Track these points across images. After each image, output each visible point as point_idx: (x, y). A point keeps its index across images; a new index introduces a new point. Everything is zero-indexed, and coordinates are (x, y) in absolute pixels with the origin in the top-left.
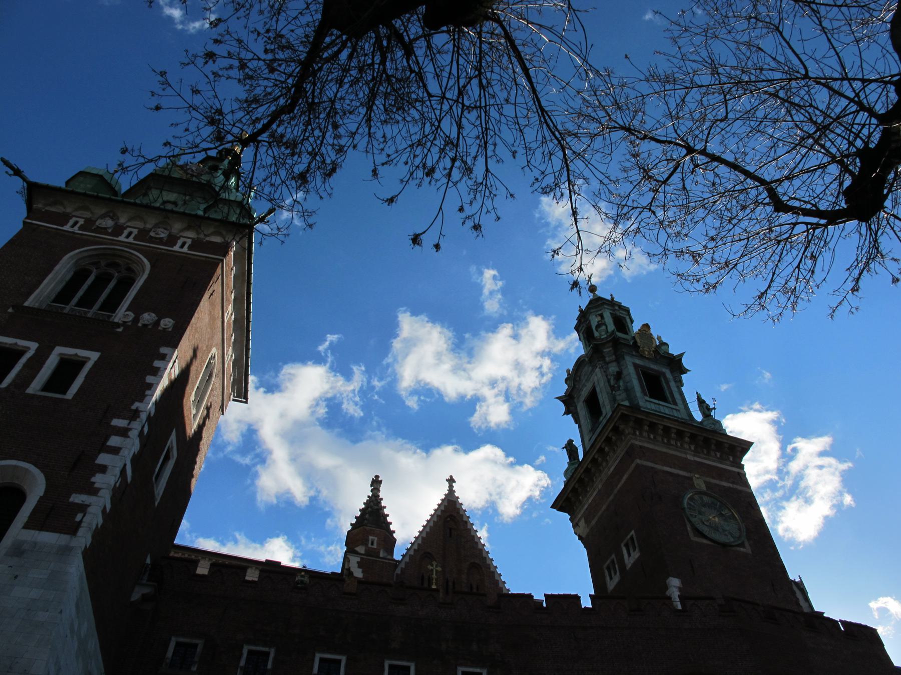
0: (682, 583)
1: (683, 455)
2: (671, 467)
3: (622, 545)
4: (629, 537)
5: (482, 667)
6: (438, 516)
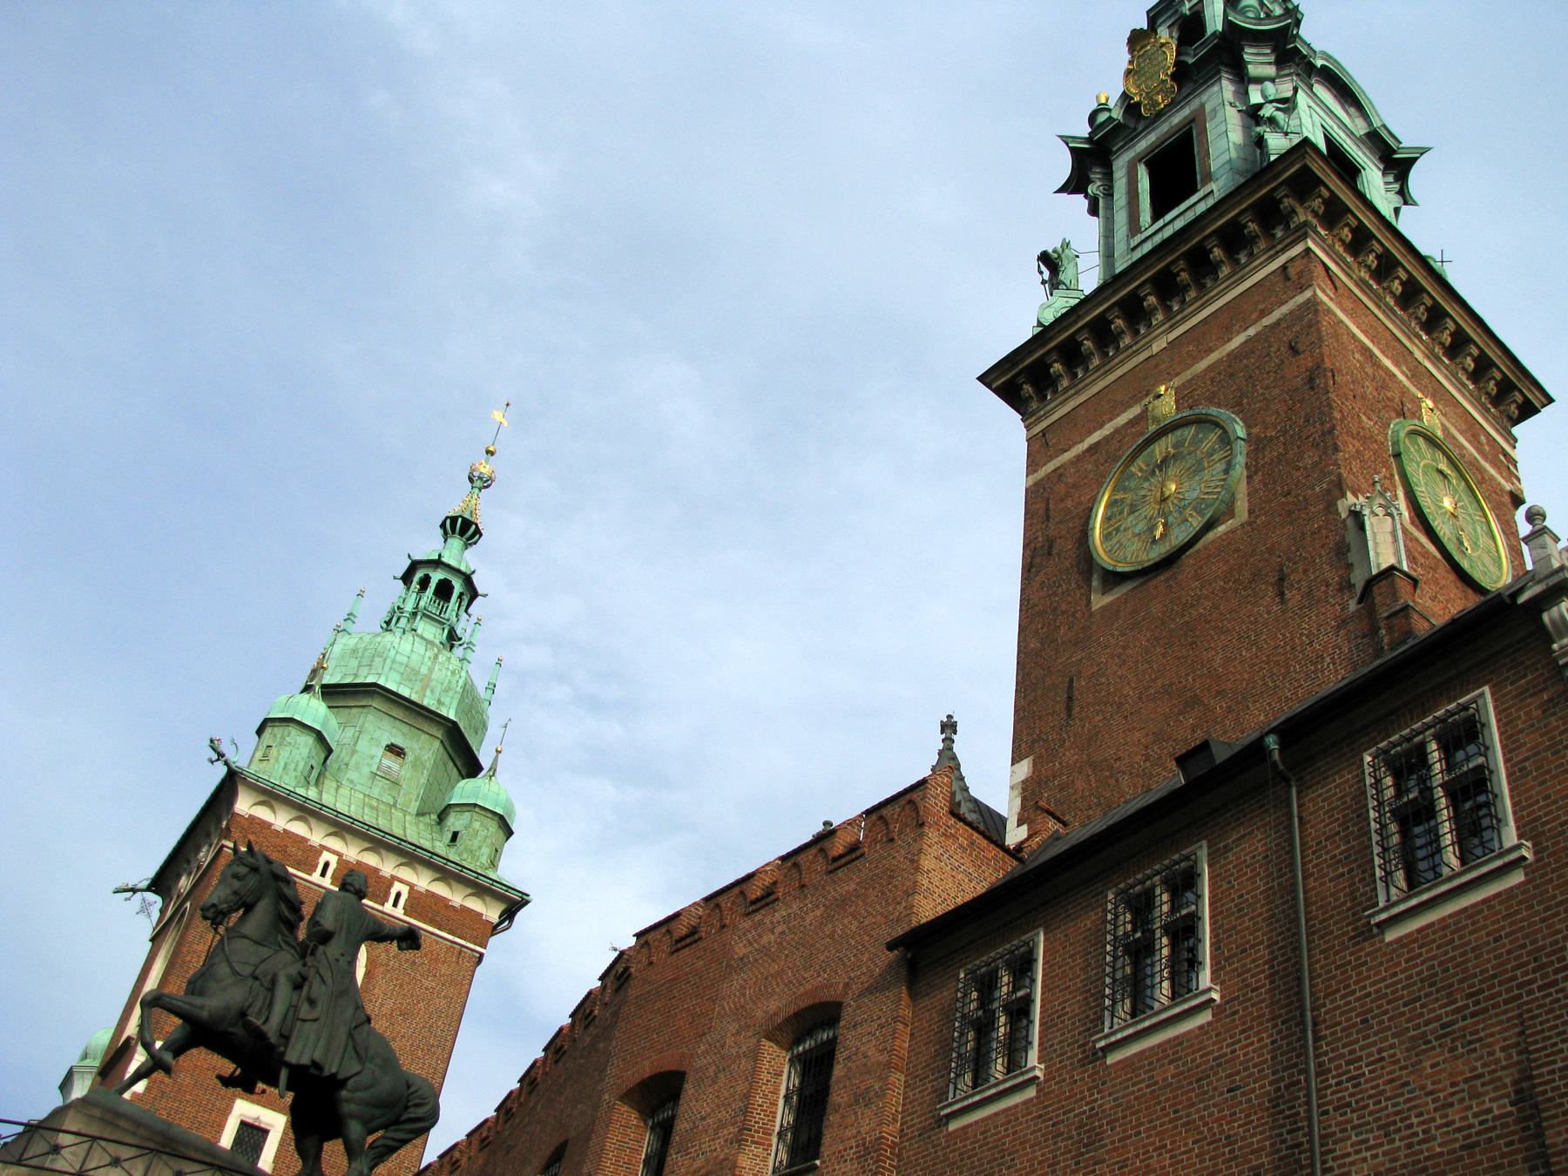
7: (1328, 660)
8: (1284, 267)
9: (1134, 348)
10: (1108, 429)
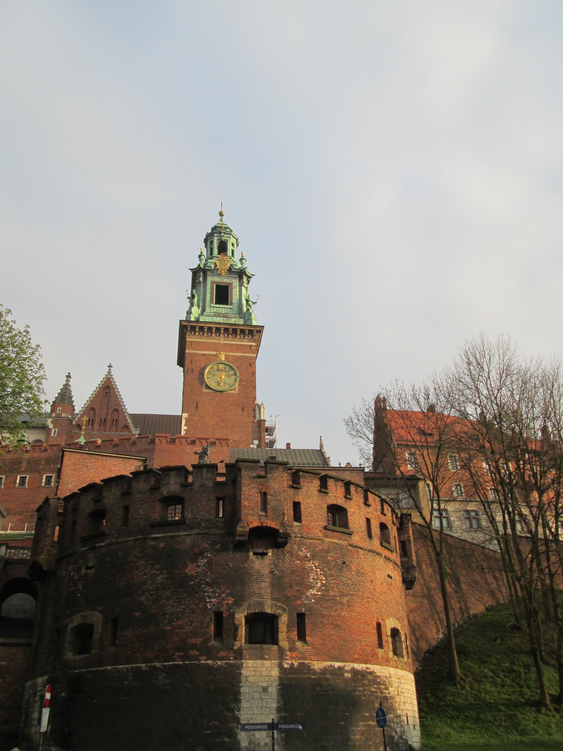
1: (217, 342)
2: (206, 351)
5: (53, 473)
6: (100, 388)
8: (250, 346)
10: (208, 353)
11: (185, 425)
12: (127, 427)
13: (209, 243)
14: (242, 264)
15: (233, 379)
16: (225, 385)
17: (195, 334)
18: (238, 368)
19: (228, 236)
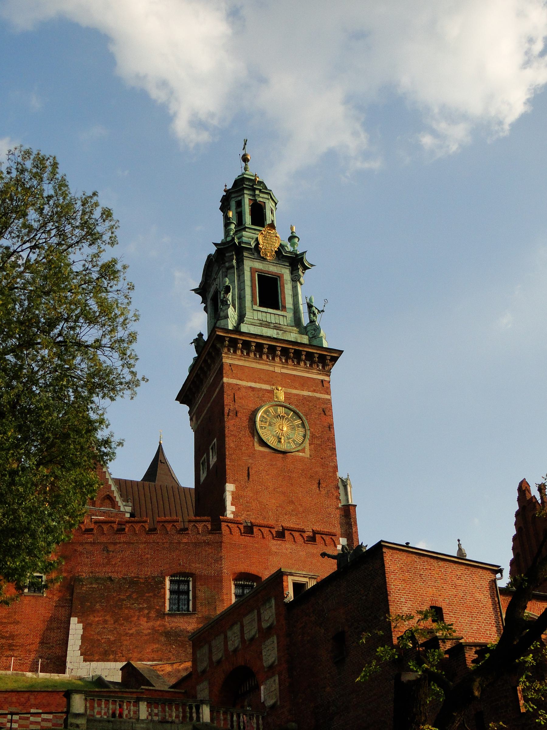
0: (236, 487)
1: (271, 369)
2: (255, 382)
3: (210, 448)
4: (213, 442)
7: (332, 516)
8: (322, 381)
9: (269, 363)
11: (232, 504)
12: (110, 498)
13: (233, 204)
14: (293, 245)
15: (302, 434)
16: (289, 443)
17: (235, 352)
18: (306, 415)
19: (266, 196)
